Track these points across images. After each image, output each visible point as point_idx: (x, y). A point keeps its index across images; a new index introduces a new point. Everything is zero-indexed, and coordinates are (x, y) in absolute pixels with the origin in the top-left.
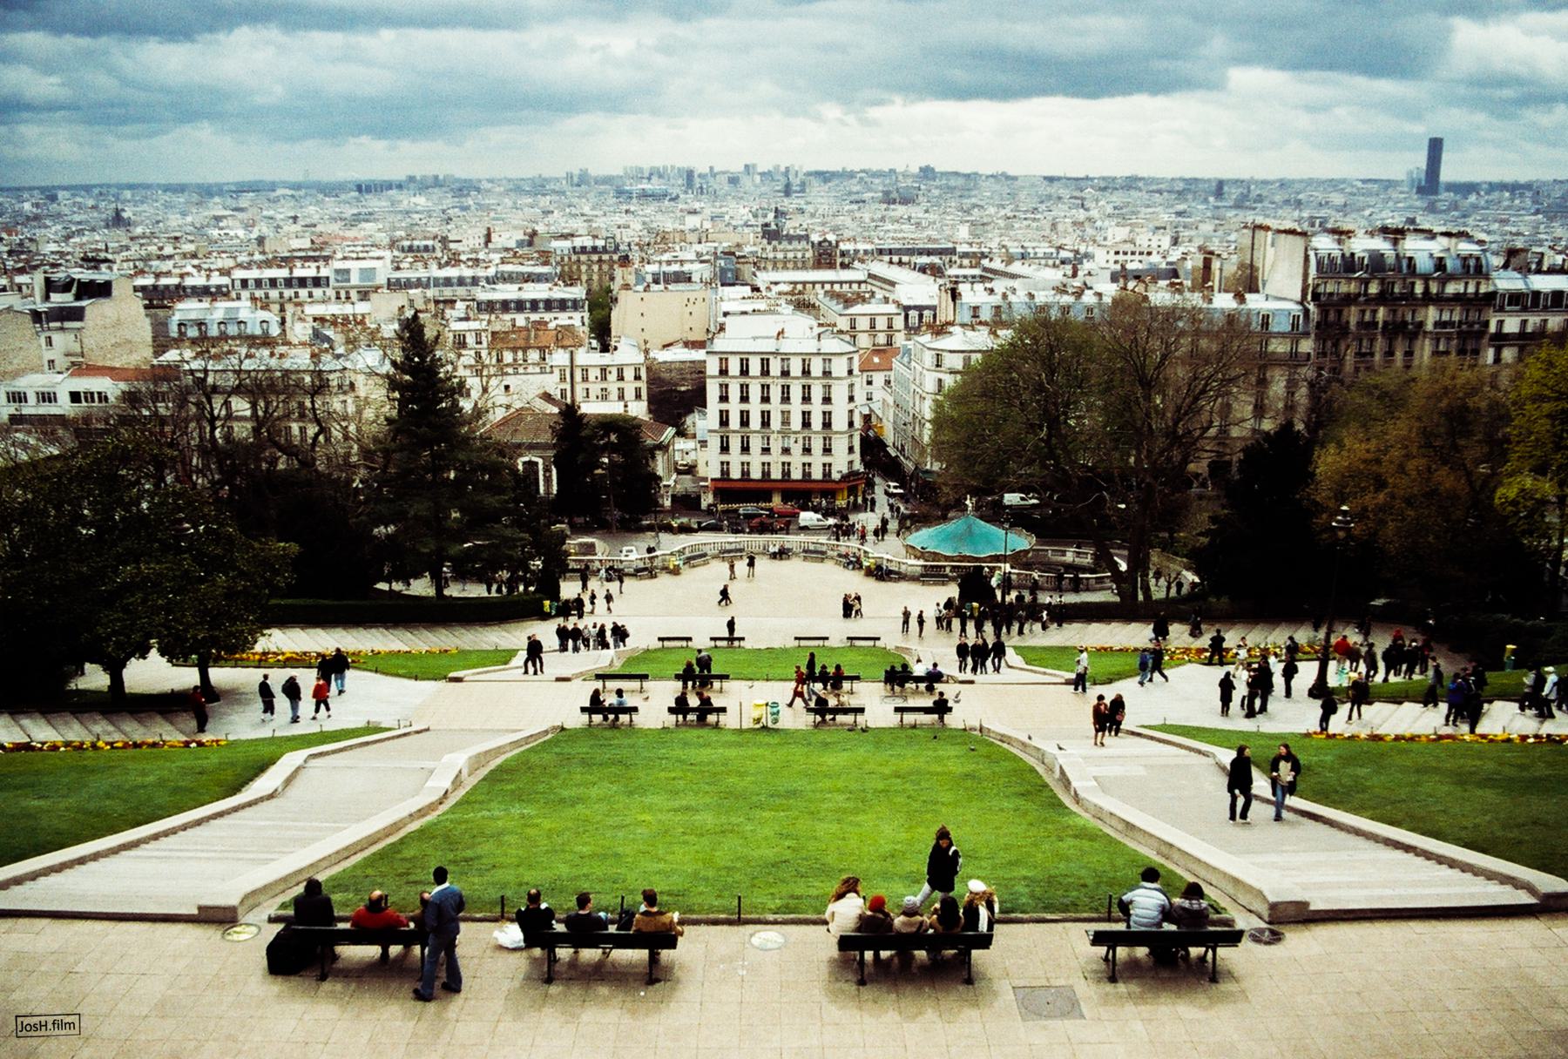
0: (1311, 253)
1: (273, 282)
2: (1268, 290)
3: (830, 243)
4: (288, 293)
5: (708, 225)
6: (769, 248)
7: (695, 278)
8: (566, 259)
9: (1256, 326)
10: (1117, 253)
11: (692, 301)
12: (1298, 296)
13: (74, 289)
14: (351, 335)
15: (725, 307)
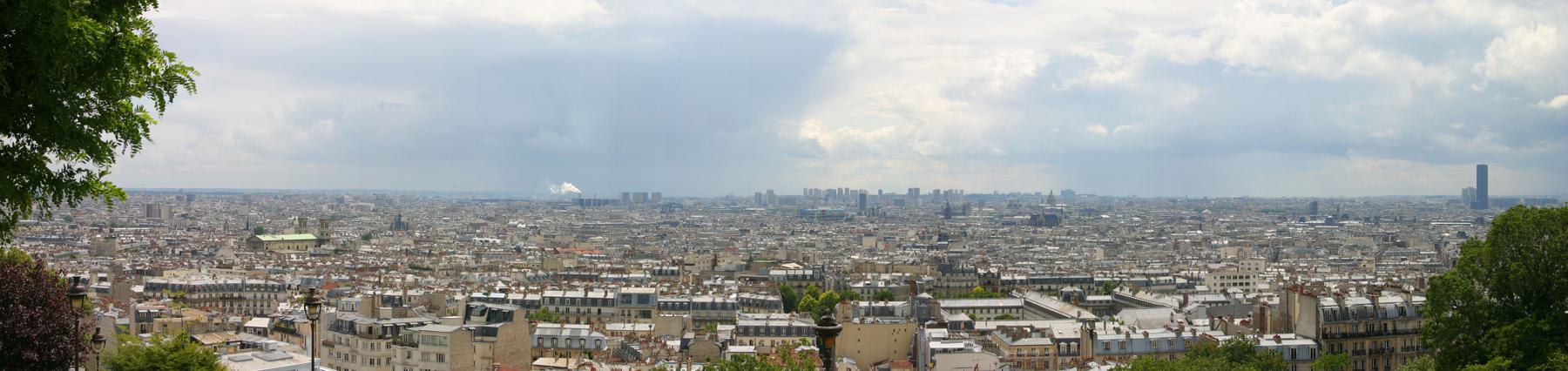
0: (1320, 309)
1: (573, 301)
2: (1300, 329)
3: (993, 274)
4: (583, 309)
5: (881, 246)
6: (943, 278)
7: (898, 313)
8: (782, 284)
9: (1287, 356)
10: (1222, 277)
11: (897, 330)
12: (1314, 335)
13: (486, 316)
14: (655, 351)
15: (934, 345)
